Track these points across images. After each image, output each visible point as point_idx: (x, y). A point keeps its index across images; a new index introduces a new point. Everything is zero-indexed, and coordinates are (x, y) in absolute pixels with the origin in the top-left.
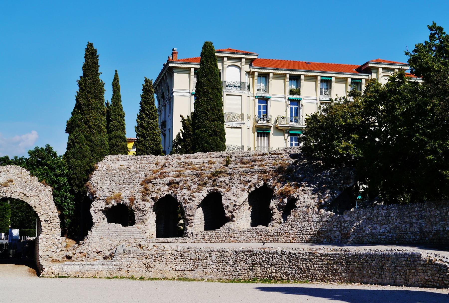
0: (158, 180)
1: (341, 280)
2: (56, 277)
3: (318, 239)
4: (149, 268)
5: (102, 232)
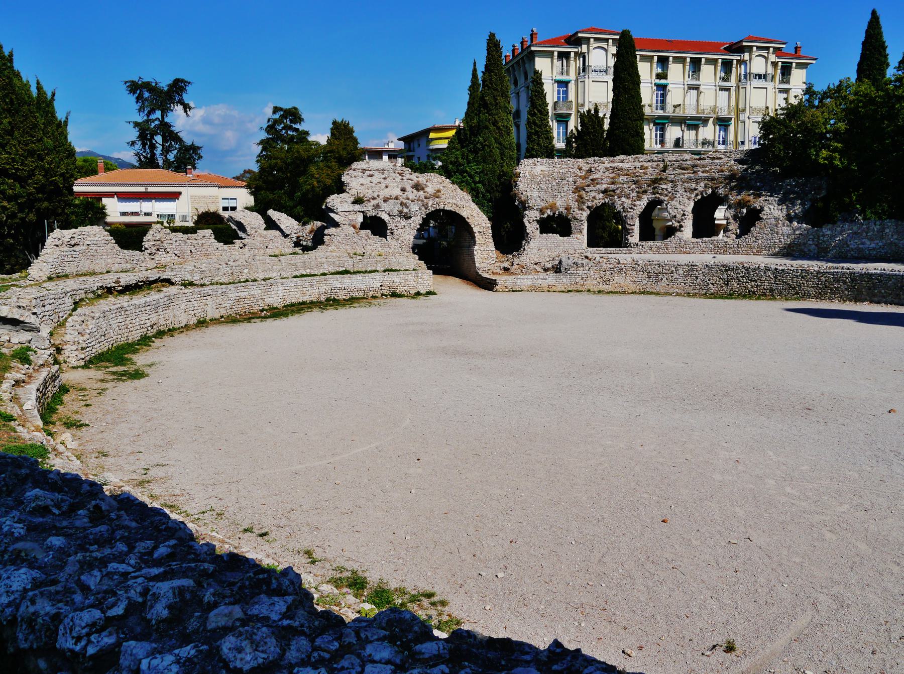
0: (591, 188)
1: (844, 298)
3: (789, 252)
4: (606, 281)
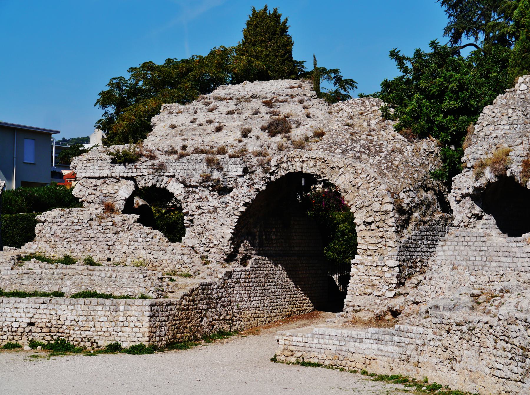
2: (298, 363)
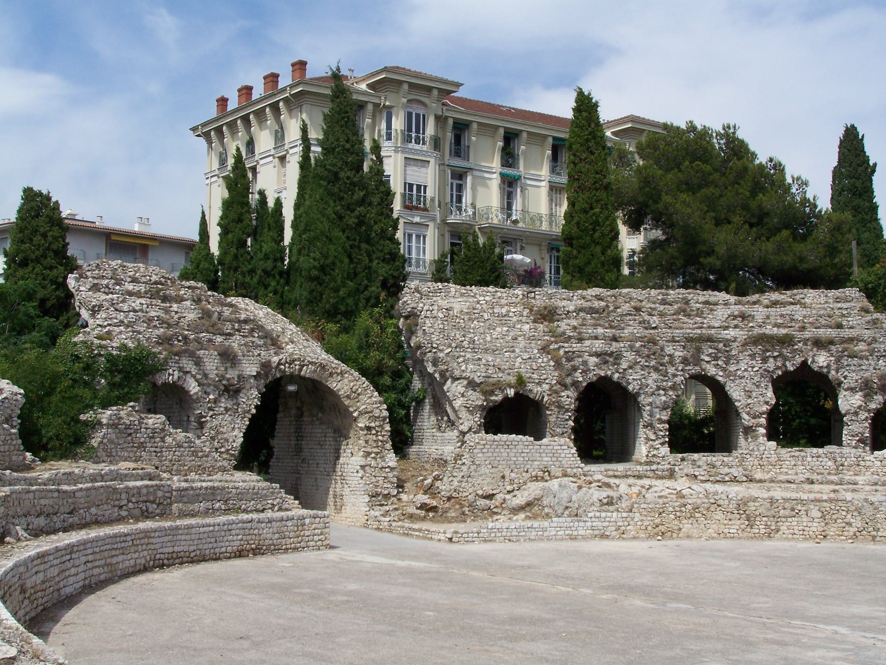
5: (495, 454)
